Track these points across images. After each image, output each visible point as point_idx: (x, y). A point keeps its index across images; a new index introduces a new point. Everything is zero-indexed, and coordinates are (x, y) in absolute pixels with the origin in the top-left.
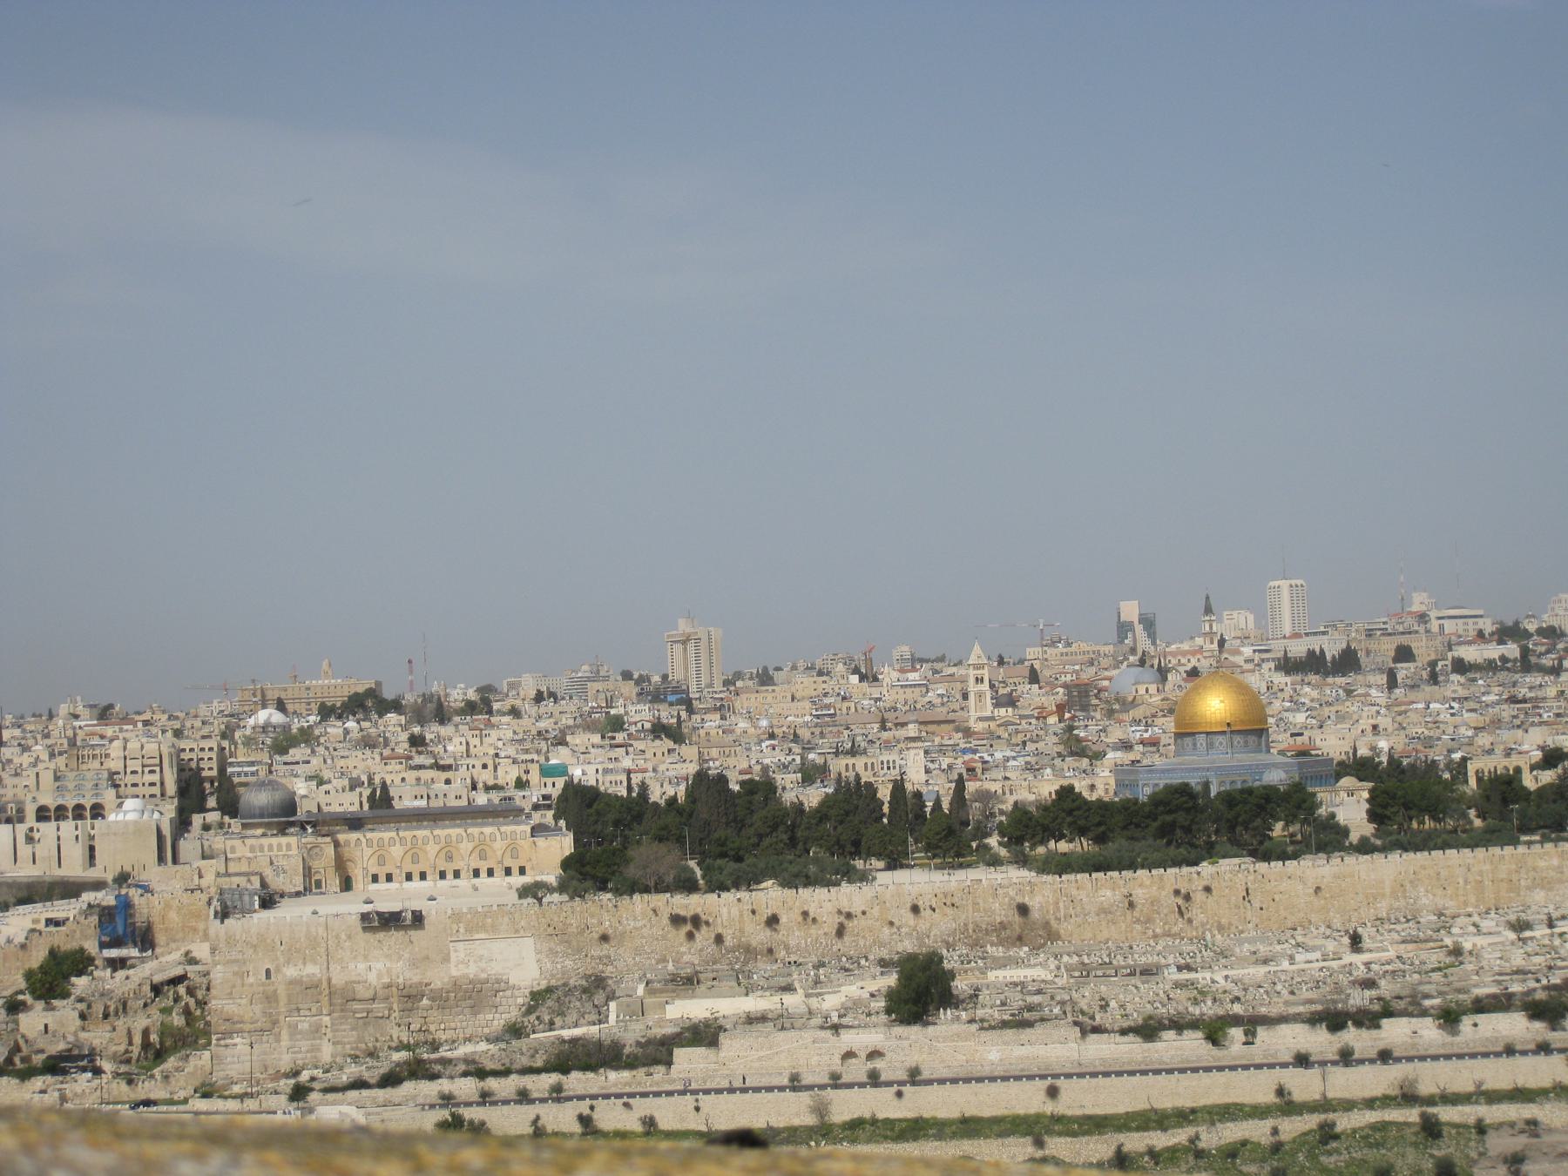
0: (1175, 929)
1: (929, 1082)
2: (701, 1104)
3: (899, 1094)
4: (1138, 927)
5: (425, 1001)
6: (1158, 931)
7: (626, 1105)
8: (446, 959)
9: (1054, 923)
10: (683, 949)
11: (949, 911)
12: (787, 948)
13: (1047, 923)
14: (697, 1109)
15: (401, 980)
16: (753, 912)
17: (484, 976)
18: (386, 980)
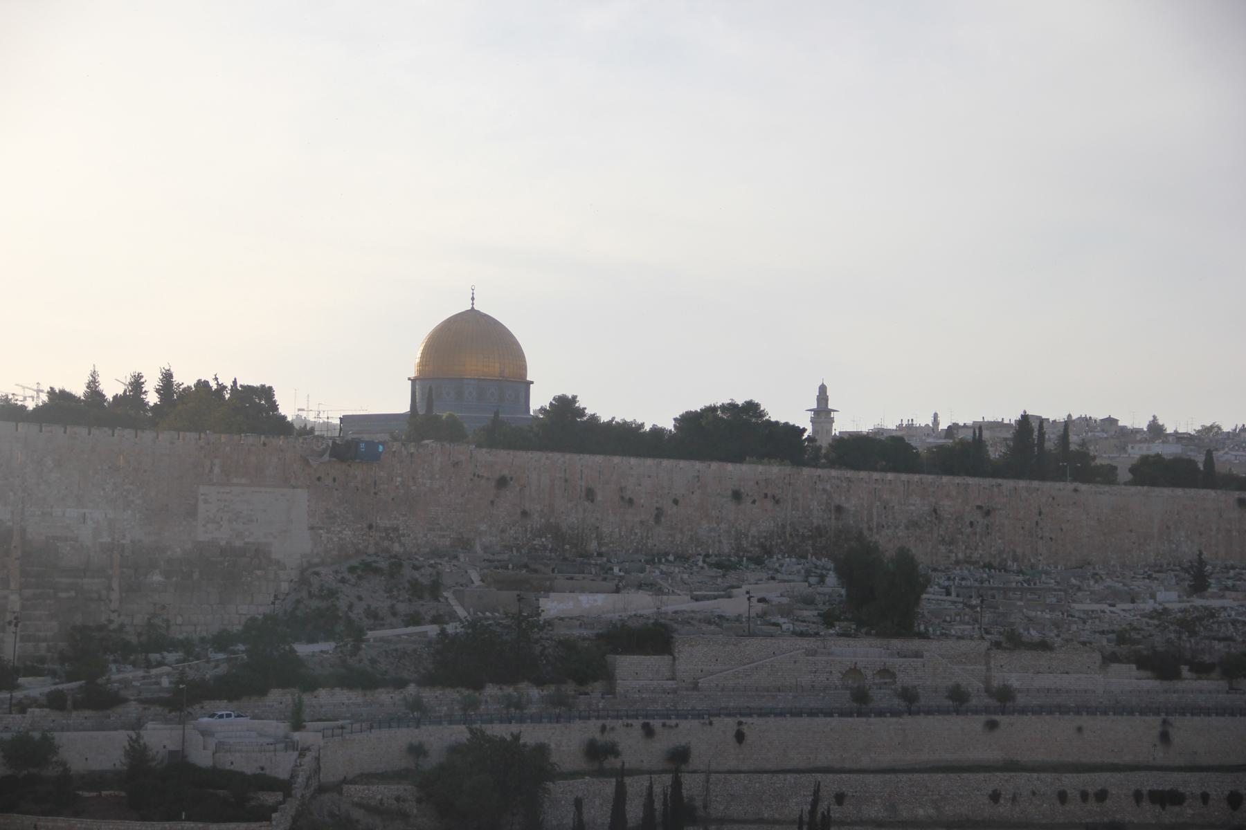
0: (976, 556)
1: (1023, 711)
2: (745, 729)
3: (992, 725)
4: (943, 549)
5: (157, 578)
6: (961, 556)
7: (649, 731)
8: (192, 513)
9: (866, 533)
10: (483, 527)
11: (769, 504)
12: (599, 538)
13: (861, 533)
14: (740, 737)
15: (126, 541)
16: (566, 481)
17: (238, 543)
18: (106, 539)
